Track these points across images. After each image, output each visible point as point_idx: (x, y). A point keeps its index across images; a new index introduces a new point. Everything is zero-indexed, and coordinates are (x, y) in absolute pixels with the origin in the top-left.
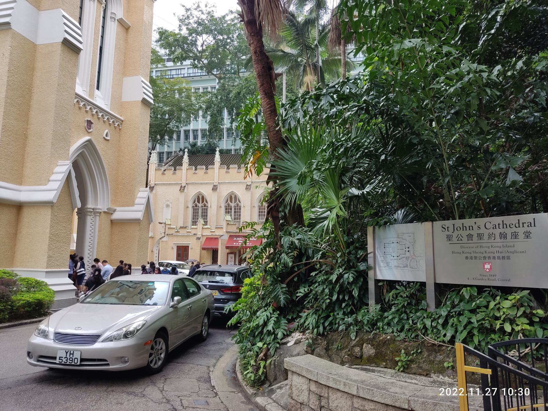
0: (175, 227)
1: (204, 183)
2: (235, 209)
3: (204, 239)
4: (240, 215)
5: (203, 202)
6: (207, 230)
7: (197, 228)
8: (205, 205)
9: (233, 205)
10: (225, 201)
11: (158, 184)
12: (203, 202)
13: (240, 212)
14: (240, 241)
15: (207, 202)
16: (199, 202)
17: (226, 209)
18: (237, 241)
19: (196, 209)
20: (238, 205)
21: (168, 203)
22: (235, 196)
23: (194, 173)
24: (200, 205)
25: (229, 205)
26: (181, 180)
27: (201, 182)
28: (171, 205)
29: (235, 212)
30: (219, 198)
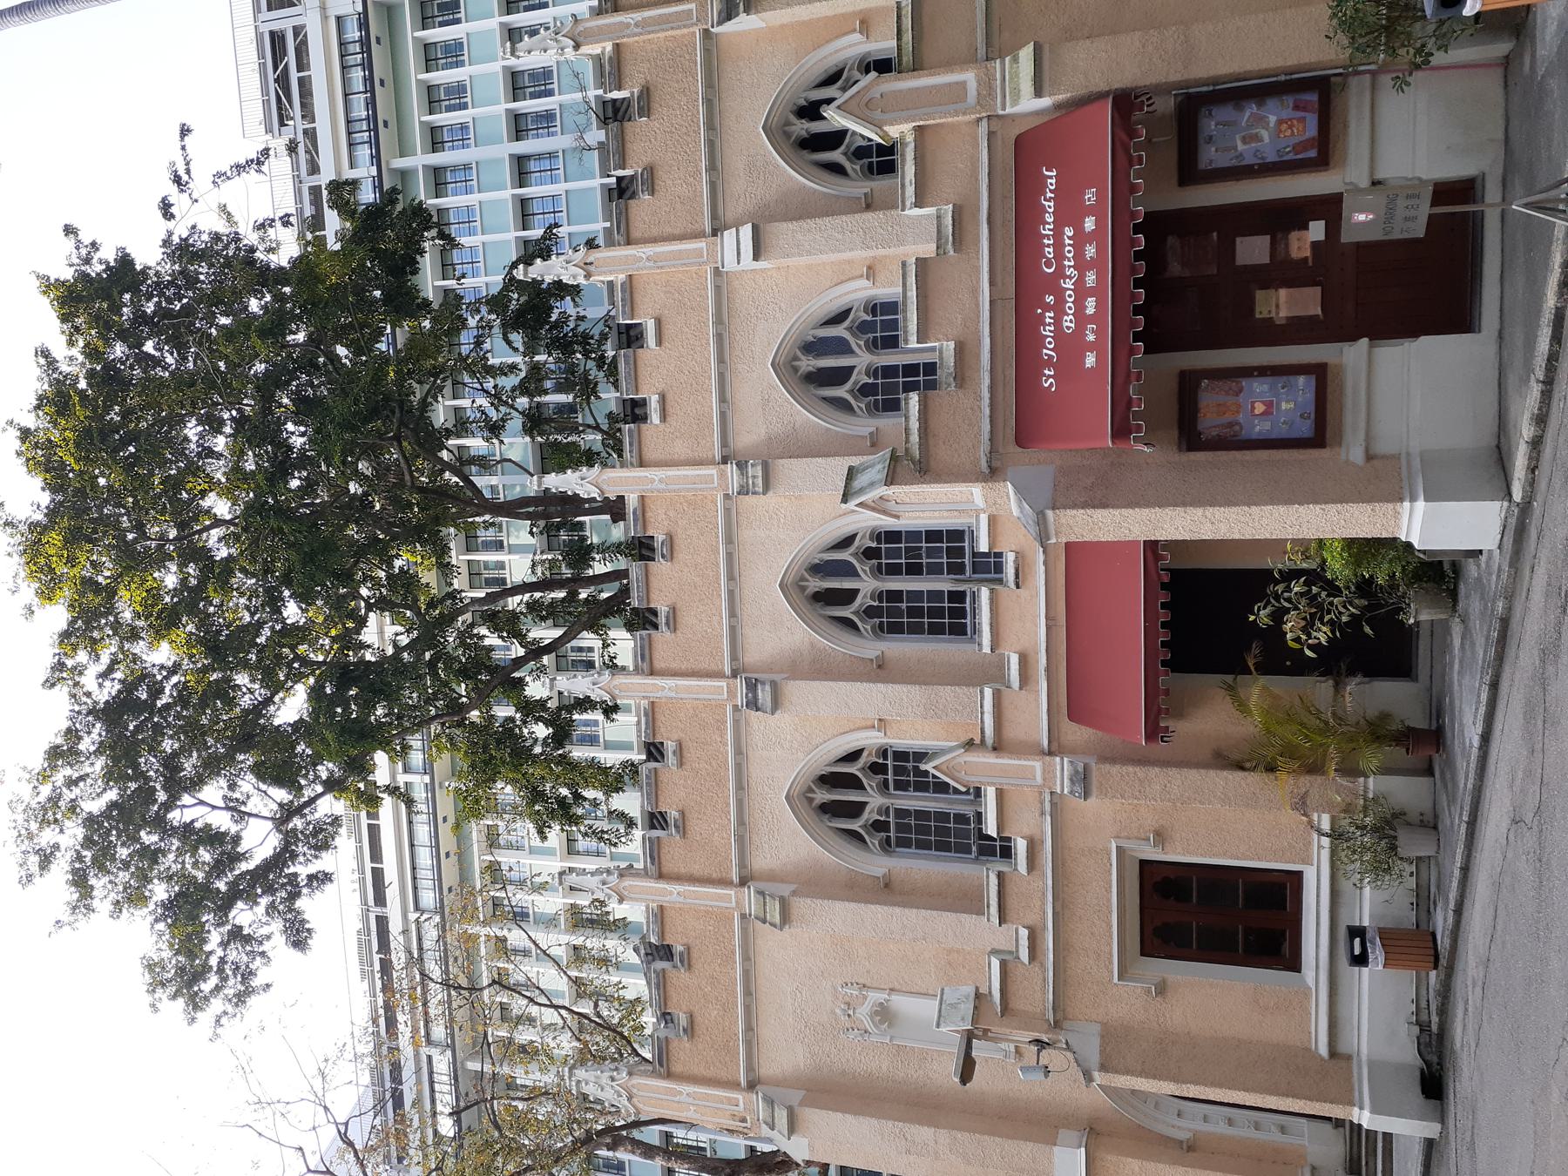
0: (996, 964)
1: (739, 767)
2: (894, 570)
3: (1075, 733)
4: (934, 535)
5: (853, 782)
6: (1009, 713)
7: (1000, 794)
8: (876, 769)
9: (867, 585)
10: (847, 636)
11: (750, 1068)
12: (853, 782)
13: (914, 535)
14: (1068, 322)
15: (853, 756)
16: (855, 810)
17: (895, 629)
18: (1070, 346)
19: (900, 828)
20: (869, 554)
21: (863, 1012)
22: (818, 569)
23: (682, 828)
24: (874, 801)
25: (870, 612)
26: (723, 918)
27: (731, 785)
28: (875, 997)
29: (914, 570)
30: (821, 669)
